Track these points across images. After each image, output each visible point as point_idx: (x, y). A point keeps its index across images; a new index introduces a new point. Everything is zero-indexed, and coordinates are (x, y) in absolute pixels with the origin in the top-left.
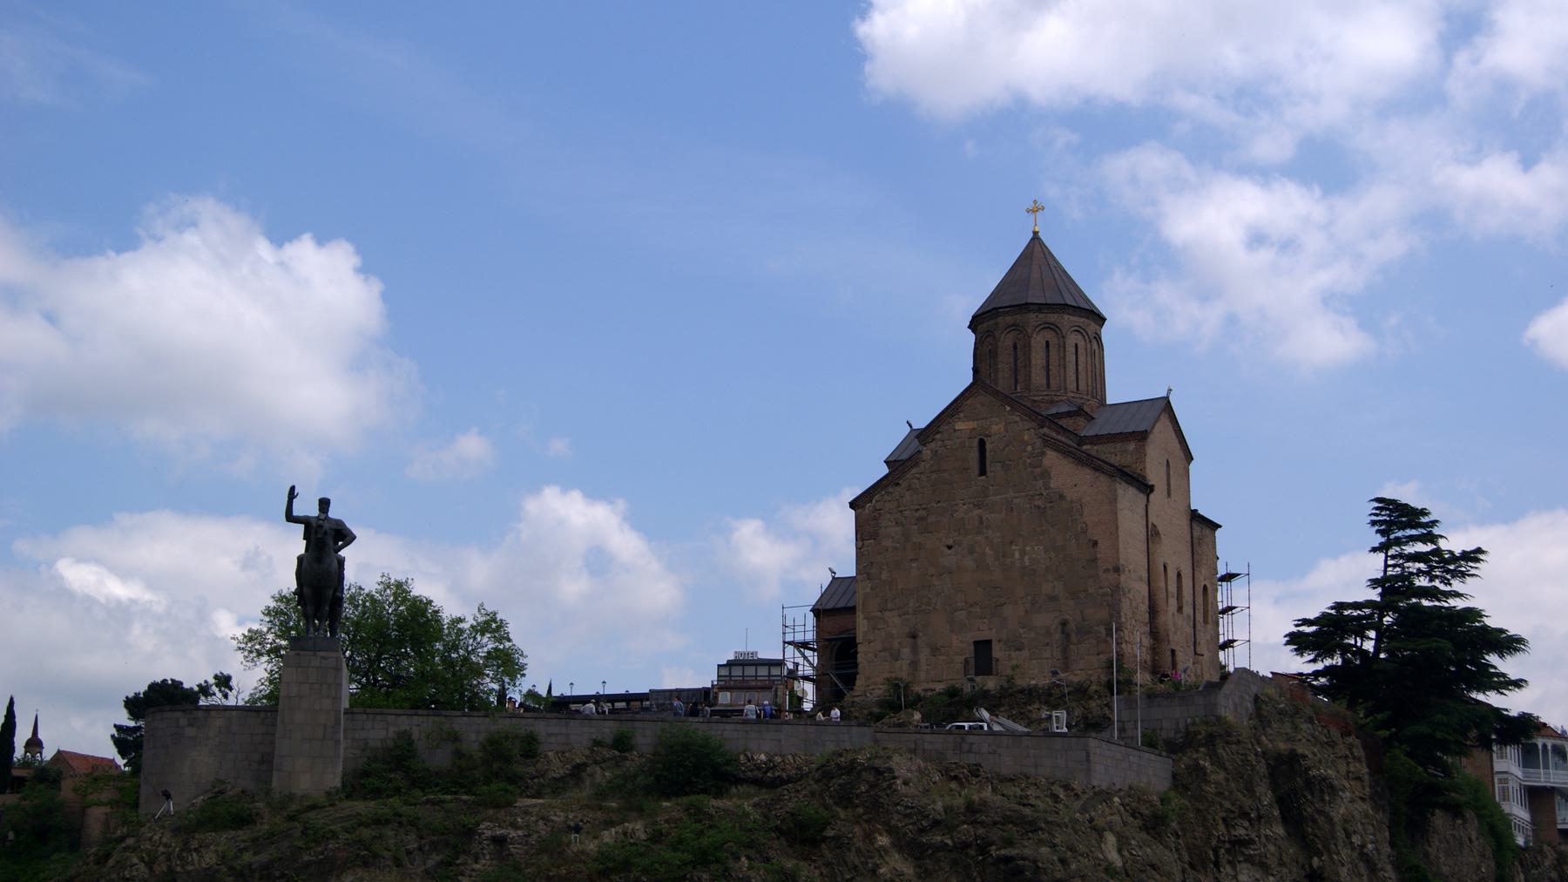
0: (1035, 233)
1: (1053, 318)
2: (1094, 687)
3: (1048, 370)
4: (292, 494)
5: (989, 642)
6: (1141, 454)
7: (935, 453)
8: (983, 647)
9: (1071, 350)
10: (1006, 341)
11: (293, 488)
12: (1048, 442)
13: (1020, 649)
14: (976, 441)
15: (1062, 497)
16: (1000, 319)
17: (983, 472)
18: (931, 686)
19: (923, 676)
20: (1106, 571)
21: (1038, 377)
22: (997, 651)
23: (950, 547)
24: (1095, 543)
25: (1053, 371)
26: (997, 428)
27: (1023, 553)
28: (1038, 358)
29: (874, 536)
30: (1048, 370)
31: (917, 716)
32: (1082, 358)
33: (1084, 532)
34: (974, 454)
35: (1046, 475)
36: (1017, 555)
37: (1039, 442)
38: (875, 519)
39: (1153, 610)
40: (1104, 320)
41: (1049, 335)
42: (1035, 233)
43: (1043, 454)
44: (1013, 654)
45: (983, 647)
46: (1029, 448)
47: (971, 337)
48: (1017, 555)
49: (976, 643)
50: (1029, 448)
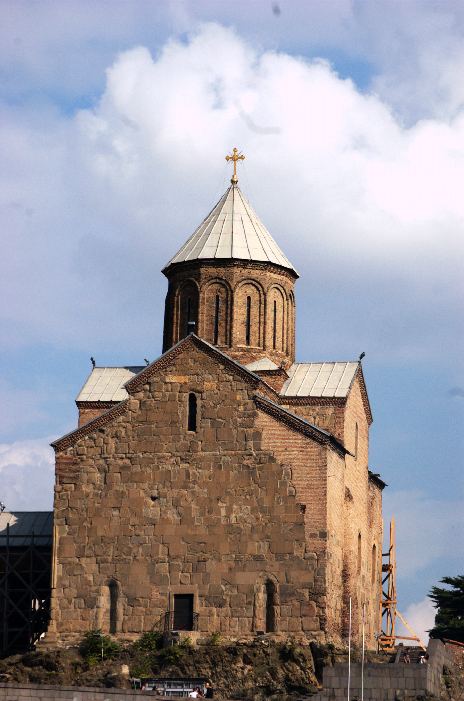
1: (256, 273)
2: (298, 650)
3: (248, 326)
5: (190, 597)
6: (339, 419)
7: (142, 403)
8: (184, 602)
9: (270, 307)
10: (207, 292)
12: (260, 404)
13: (220, 606)
14: (186, 397)
15: (272, 459)
16: (203, 270)
18: (127, 636)
19: (119, 626)
21: (238, 332)
22: (198, 607)
23: (154, 499)
24: (304, 508)
25: (254, 328)
26: (209, 385)
27: (229, 510)
28: (239, 314)
29: (75, 481)
30: (248, 326)
31: (126, 670)
32: (279, 315)
33: (293, 496)
35: (258, 435)
36: (223, 513)
38: (76, 463)
39: (345, 575)
40: (297, 277)
41: (252, 291)
43: (255, 415)
44: (214, 610)
45: (184, 602)
46: (241, 408)
47: (165, 282)
48: (223, 513)
49: (176, 596)
50: (241, 408)
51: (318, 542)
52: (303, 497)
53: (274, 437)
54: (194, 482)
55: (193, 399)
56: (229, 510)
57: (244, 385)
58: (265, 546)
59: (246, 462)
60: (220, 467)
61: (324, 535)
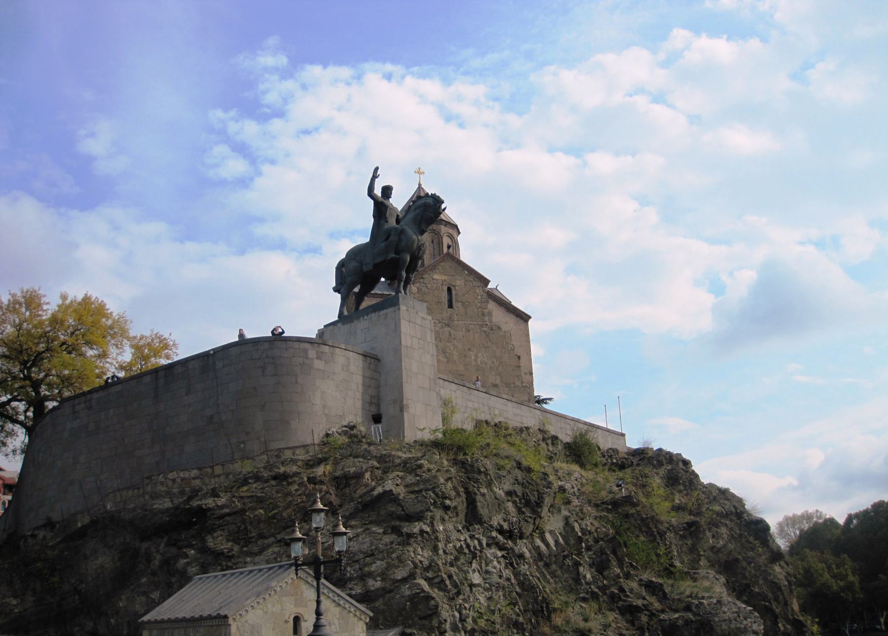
0: (420, 185)
1: (451, 231)
4: (375, 176)
11: (377, 169)
15: (499, 328)
17: (450, 306)
20: (525, 374)
24: (519, 357)
26: (459, 282)
27: (477, 356)
34: (445, 294)
35: (490, 314)
36: (473, 358)
37: (485, 295)
42: (420, 185)
43: (487, 302)
50: (479, 297)
51: (528, 377)
52: (519, 351)
53: (498, 316)
54: (455, 339)
55: (449, 290)
56: (477, 356)
57: (479, 284)
58: (499, 379)
59: (484, 329)
60: (469, 331)
61: (531, 374)
